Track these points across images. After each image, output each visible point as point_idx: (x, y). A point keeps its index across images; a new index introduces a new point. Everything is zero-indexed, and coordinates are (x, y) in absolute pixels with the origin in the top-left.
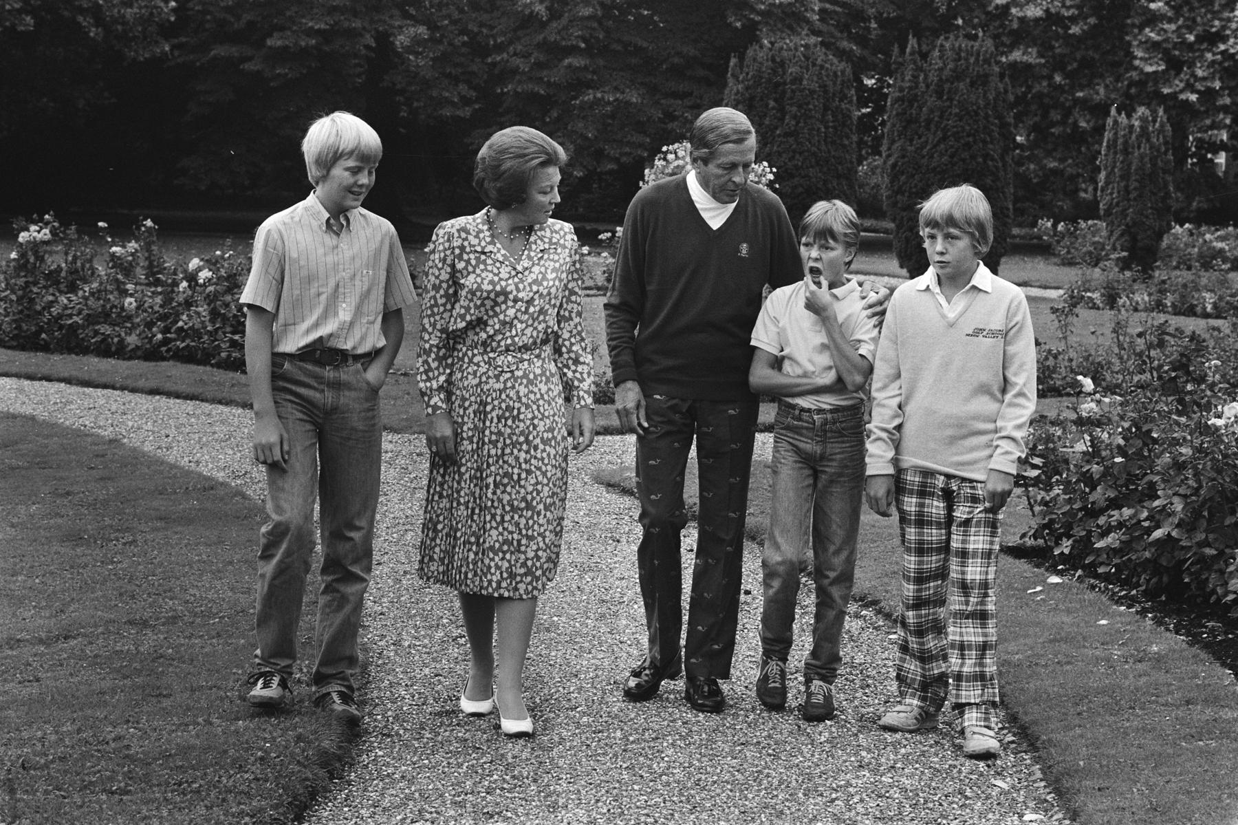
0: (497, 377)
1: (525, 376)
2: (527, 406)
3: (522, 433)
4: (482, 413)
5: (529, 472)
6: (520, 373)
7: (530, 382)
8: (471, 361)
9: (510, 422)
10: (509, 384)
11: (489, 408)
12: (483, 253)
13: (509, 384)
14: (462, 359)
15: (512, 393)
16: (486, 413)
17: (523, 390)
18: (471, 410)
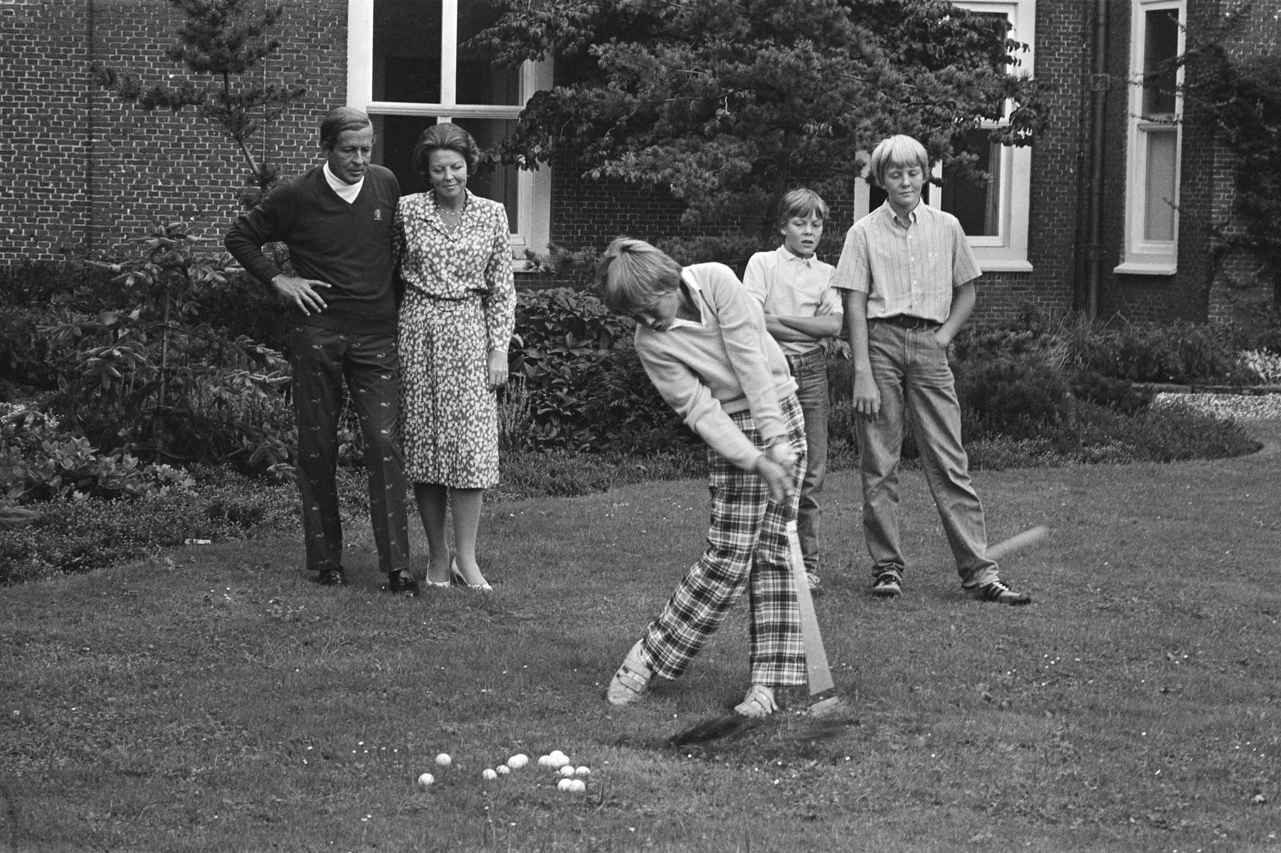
0: (440, 315)
1: (462, 315)
2: (464, 340)
3: (460, 360)
4: (429, 342)
5: (465, 390)
6: (458, 313)
7: (466, 321)
8: (419, 303)
9: (451, 350)
10: (449, 321)
11: (435, 339)
12: (426, 221)
13: (449, 321)
14: (412, 302)
15: (452, 329)
16: (433, 343)
17: (460, 327)
18: (420, 341)
